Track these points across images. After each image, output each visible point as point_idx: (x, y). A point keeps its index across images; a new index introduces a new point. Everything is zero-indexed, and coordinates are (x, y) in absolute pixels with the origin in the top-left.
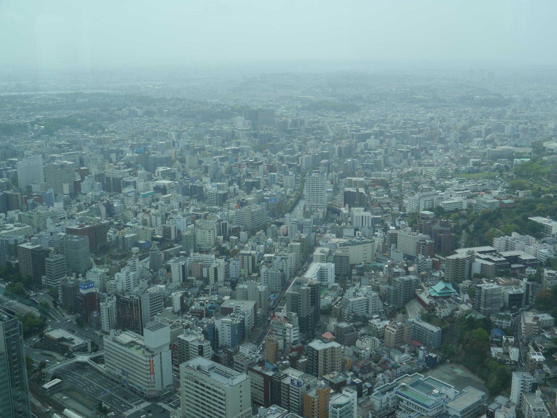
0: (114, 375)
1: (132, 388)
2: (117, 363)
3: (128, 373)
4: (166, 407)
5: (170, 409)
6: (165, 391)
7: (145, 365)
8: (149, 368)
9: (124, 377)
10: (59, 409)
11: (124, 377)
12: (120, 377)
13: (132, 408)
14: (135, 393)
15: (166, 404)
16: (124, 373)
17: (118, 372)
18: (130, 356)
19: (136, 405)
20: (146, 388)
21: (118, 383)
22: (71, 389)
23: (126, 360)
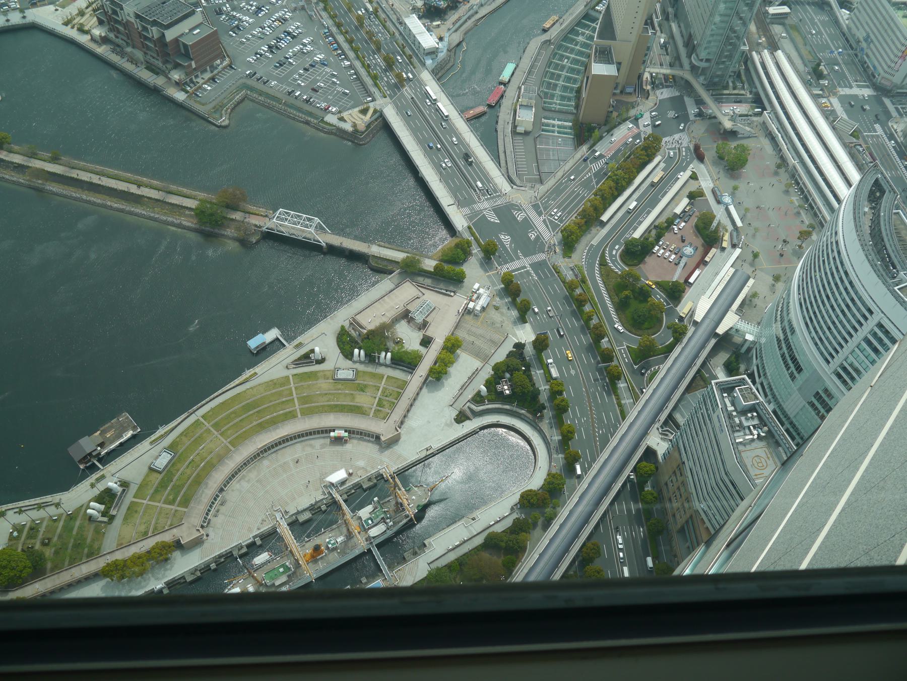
0: (853, 36)
1: (866, 62)
2: (867, 23)
3: (872, 41)
4: (891, 107)
5: (894, 114)
6: (901, 88)
7: (901, 43)
8: (903, 49)
9: (864, 45)
10: (773, 47)
11: (864, 45)
12: (858, 42)
13: (851, 87)
14: (865, 70)
15: (893, 104)
16: (867, 39)
17: (861, 35)
18: (890, 21)
19: (859, 86)
20: (881, 72)
21: (852, 48)
22: (795, 28)
23: (881, 23)
